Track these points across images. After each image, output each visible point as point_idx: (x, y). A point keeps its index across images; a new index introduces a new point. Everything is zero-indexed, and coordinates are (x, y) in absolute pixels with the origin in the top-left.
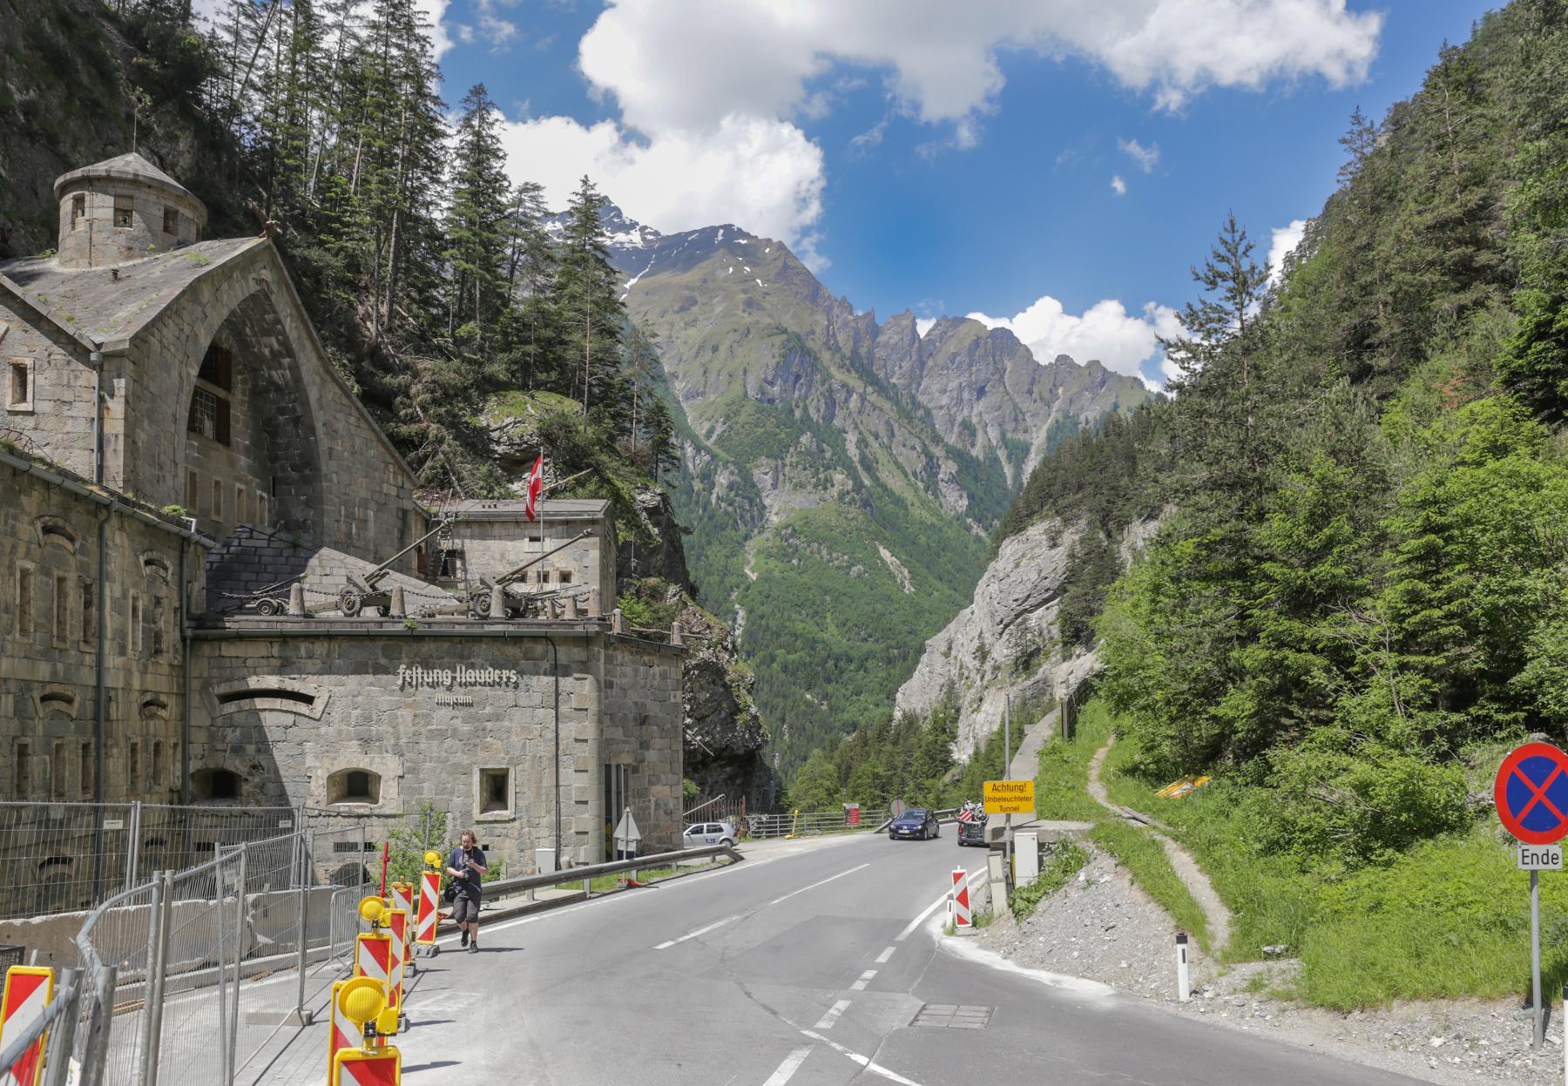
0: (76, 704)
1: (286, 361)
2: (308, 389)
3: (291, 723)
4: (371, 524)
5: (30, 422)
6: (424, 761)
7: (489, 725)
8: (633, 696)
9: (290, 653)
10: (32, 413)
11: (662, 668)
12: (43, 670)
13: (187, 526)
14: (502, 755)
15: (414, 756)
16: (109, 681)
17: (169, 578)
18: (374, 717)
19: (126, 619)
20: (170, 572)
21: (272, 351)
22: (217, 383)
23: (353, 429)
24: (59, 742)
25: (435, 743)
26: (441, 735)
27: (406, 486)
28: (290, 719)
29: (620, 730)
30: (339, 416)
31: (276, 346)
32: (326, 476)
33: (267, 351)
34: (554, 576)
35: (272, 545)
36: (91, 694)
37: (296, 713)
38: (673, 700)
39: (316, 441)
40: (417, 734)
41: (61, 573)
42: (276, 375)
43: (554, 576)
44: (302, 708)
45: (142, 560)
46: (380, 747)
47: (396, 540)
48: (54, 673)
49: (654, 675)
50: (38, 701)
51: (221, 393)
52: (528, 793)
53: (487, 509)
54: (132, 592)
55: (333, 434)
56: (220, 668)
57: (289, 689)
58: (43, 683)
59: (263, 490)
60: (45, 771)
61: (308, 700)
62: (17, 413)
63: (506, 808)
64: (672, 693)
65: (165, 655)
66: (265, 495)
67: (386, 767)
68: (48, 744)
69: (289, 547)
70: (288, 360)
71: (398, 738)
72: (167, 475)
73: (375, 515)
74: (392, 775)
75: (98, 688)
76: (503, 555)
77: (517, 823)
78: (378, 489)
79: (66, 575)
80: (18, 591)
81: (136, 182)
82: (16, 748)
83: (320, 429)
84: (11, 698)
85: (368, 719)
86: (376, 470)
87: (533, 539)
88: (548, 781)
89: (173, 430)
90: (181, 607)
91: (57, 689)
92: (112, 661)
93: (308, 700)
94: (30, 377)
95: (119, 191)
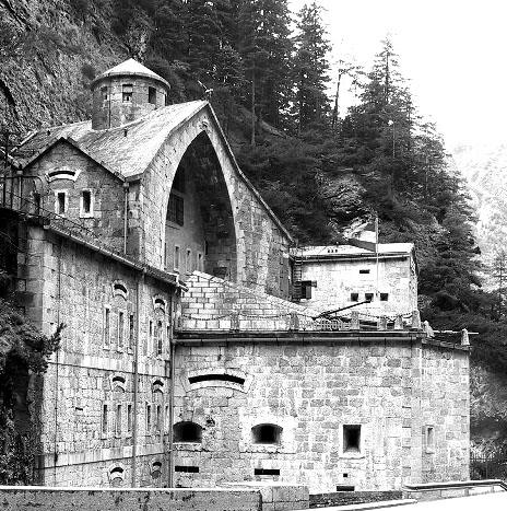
7: (349, 397)
9: (231, 353)
26: (319, 403)
28: (230, 393)
44: (237, 386)
45: (154, 299)
61: (241, 381)
63: (359, 450)
71: (293, 405)
77: (365, 460)
81: (134, 77)
91: (118, 374)
92: (141, 359)
93: (241, 381)
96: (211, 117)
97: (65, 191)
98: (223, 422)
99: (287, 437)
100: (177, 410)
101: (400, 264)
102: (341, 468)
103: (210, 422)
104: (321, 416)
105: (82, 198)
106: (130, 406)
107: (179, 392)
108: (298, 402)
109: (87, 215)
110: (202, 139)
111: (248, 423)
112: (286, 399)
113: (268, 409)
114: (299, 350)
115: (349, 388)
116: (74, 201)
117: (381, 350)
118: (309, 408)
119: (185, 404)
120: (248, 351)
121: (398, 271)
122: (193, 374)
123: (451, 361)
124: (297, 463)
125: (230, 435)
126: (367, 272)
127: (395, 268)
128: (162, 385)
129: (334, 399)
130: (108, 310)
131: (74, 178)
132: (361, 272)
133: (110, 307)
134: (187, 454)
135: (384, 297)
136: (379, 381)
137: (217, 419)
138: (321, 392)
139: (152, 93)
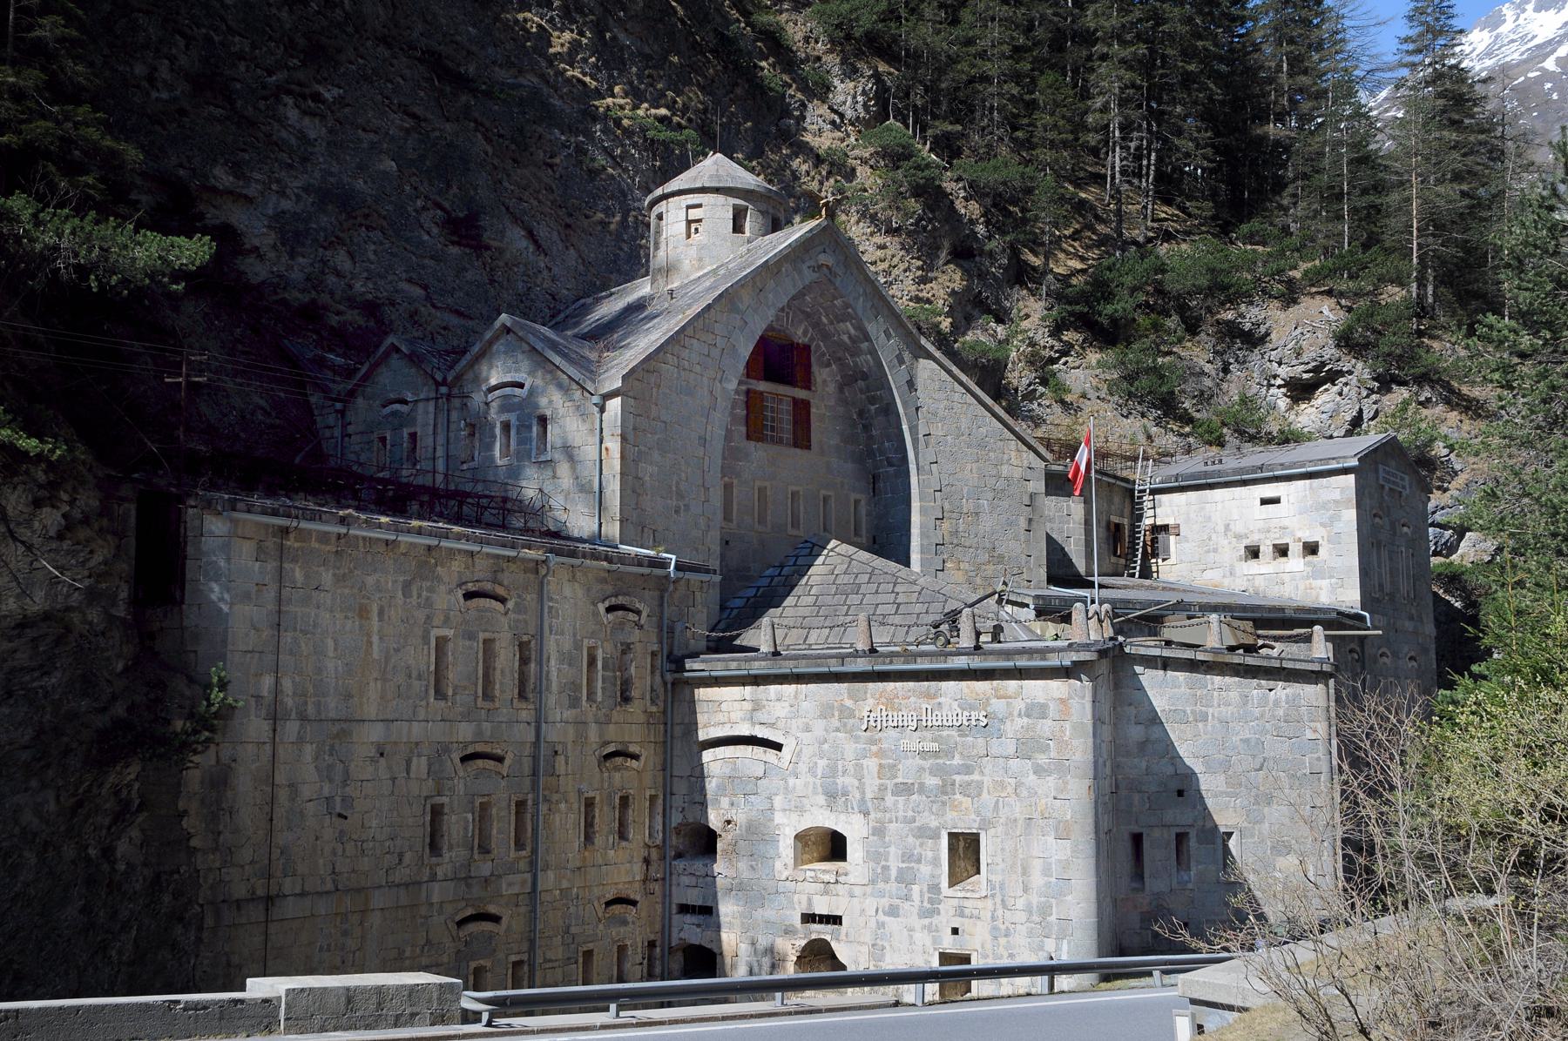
0: (507, 762)
1: (865, 345)
3: (761, 774)
7: (958, 778)
12: (465, 731)
13: (664, 564)
16: (551, 734)
20: (644, 614)
21: (850, 337)
22: (789, 381)
24: (485, 799)
26: (905, 789)
31: (852, 331)
34: (1295, 549)
40: (882, 788)
41: (487, 635)
42: (861, 360)
43: (1295, 549)
44: (770, 755)
45: (602, 607)
48: (479, 733)
50: (457, 761)
51: (801, 394)
58: (466, 745)
60: (466, 829)
61: (778, 747)
65: (636, 702)
67: (853, 829)
71: (863, 793)
75: (536, 743)
76: (1227, 527)
80: (433, 658)
82: (428, 807)
84: (424, 759)
85: (832, 771)
91: (480, 748)
93: (778, 747)
95: (690, 202)
99: (854, 850)
100: (678, 801)
102: (946, 920)
104: (910, 813)
106: (521, 805)
108: (872, 784)
111: (788, 826)
112: (848, 781)
113: (821, 799)
115: (957, 761)
118: (890, 799)
124: (871, 904)
126: (1275, 501)
128: (635, 757)
129: (932, 781)
130: (441, 643)
132: (1264, 502)
133: (449, 633)
134: (693, 881)
135: (1311, 549)
138: (907, 770)
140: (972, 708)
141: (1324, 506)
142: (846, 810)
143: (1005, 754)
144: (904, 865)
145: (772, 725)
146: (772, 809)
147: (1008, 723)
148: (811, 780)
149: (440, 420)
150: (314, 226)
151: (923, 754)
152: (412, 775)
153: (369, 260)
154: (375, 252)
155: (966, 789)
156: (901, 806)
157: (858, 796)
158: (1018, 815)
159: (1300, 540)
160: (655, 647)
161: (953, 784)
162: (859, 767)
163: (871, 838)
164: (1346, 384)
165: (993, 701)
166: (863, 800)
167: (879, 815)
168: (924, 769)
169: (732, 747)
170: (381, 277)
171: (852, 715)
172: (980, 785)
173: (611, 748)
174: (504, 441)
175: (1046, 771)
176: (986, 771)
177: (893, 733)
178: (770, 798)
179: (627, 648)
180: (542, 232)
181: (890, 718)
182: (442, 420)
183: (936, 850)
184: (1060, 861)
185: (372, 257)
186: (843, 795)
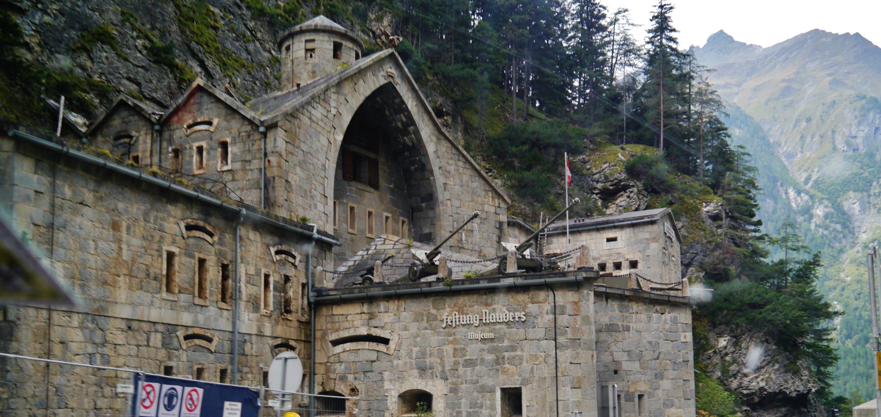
0: (215, 343)
2: (427, 145)
4: (476, 233)
5: (230, 177)
6: (462, 383)
7: (506, 354)
8: (647, 337)
9: (374, 309)
10: (230, 171)
11: (673, 315)
14: (517, 377)
15: (454, 380)
17: (297, 264)
18: (428, 352)
19: (260, 289)
20: (298, 259)
23: (461, 170)
24: (200, 367)
25: (469, 369)
26: (470, 363)
27: (501, 206)
29: (637, 364)
30: (450, 162)
31: (404, 119)
32: (442, 202)
33: (399, 124)
34: (625, 264)
35: (396, 247)
36: (228, 336)
37: (378, 351)
38: (683, 340)
39: (434, 179)
40: (456, 363)
43: (625, 264)
44: (382, 347)
45: (273, 250)
46: (432, 373)
47: (495, 243)
48: (196, 321)
49: (666, 320)
50: (181, 338)
52: (536, 406)
53: (578, 223)
54: (264, 271)
55: (446, 173)
56: (332, 322)
57: (374, 334)
59: (387, 211)
61: (386, 341)
62: (223, 172)
64: (682, 334)
65: (294, 314)
66: (389, 215)
67: (436, 388)
68: (191, 367)
69: (406, 248)
70: (412, 127)
71: (443, 367)
72: (318, 204)
73: (479, 227)
74: (440, 393)
78: (481, 208)
79: (206, 257)
83: (436, 171)
84: (159, 336)
85: (423, 354)
86: (479, 196)
87: (609, 240)
88: (551, 398)
89: (323, 176)
90: (308, 283)
91: (197, 331)
93: (386, 341)
94: (229, 149)
96: (398, 66)
97: (204, 144)
98: (367, 391)
99: (438, 404)
101: (649, 228)
103: (354, 391)
104: (475, 378)
105: (220, 150)
107: (320, 357)
108: (449, 361)
109: (225, 168)
110: (387, 92)
111: (393, 391)
113: (415, 372)
114: (449, 302)
115: (506, 343)
116: (212, 153)
117: (542, 295)
118: (461, 370)
119: (328, 371)
120: (392, 305)
121: (647, 236)
122: (334, 337)
123: (668, 316)
125: (375, 405)
126: (614, 239)
127: (645, 233)
129: (490, 357)
131: (212, 129)
132: (609, 240)
135: (634, 264)
136: (541, 333)
137: (361, 387)
139: (337, 48)
140: (515, 311)
141: (640, 242)
142: (433, 376)
143: (538, 337)
144: (471, 410)
145: (382, 328)
146: (382, 380)
147: (540, 319)
148: (408, 360)
149: (154, 147)
150: (66, 35)
151: (484, 340)
152: (151, 344)
153: (103, 63)
154: (107, 58)
155: (511, 361)
156: (469, 373)
157: (440, 369)
158: (546, 375)
159: (627, 260)
160: (304, 281)
161: (503, 358)
162: (440, 351)
163: (449, 394)
164: (631, 192)
165: (530, 305)
166: (443, 371)
167: (454, 380)
168: (483, 350)
169: (355, 344)
170: (110, 74)
171: (435, 319)
172: (521, 358)
173: (279, 341)
174: (198, 159)
175: (564, 346)
176: (526, 349)
177: (464, 329)
178: (381, 373)
179: (287, 279)
180: (209, 63)
181: (461, 320)
182: (157, 147)
183: (493, 400)
184: (575, 402)
185: (105, 60)
186: (430, 369)
